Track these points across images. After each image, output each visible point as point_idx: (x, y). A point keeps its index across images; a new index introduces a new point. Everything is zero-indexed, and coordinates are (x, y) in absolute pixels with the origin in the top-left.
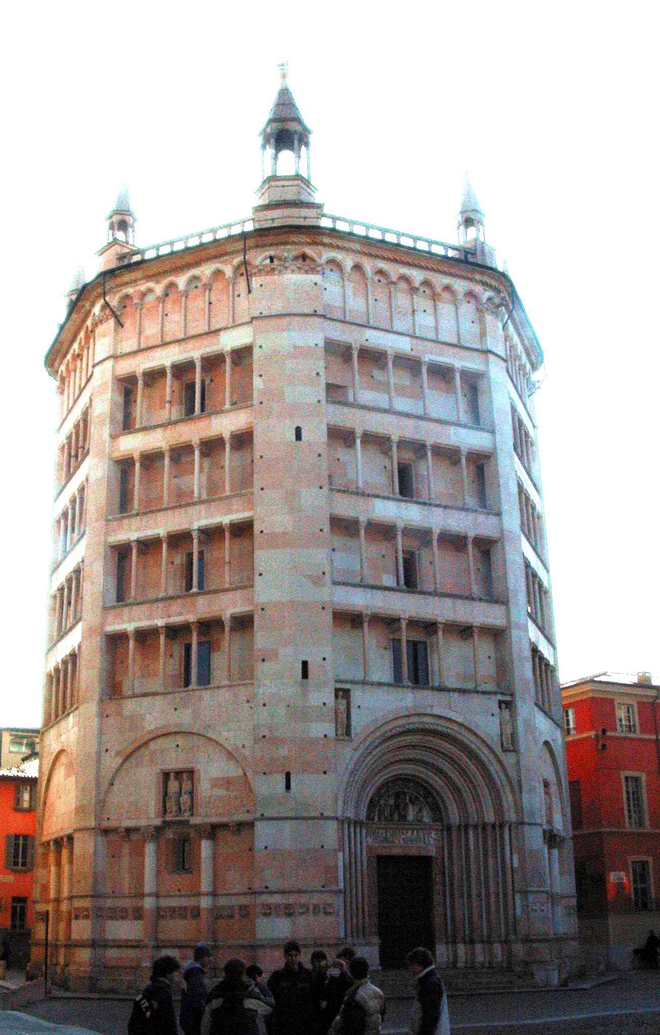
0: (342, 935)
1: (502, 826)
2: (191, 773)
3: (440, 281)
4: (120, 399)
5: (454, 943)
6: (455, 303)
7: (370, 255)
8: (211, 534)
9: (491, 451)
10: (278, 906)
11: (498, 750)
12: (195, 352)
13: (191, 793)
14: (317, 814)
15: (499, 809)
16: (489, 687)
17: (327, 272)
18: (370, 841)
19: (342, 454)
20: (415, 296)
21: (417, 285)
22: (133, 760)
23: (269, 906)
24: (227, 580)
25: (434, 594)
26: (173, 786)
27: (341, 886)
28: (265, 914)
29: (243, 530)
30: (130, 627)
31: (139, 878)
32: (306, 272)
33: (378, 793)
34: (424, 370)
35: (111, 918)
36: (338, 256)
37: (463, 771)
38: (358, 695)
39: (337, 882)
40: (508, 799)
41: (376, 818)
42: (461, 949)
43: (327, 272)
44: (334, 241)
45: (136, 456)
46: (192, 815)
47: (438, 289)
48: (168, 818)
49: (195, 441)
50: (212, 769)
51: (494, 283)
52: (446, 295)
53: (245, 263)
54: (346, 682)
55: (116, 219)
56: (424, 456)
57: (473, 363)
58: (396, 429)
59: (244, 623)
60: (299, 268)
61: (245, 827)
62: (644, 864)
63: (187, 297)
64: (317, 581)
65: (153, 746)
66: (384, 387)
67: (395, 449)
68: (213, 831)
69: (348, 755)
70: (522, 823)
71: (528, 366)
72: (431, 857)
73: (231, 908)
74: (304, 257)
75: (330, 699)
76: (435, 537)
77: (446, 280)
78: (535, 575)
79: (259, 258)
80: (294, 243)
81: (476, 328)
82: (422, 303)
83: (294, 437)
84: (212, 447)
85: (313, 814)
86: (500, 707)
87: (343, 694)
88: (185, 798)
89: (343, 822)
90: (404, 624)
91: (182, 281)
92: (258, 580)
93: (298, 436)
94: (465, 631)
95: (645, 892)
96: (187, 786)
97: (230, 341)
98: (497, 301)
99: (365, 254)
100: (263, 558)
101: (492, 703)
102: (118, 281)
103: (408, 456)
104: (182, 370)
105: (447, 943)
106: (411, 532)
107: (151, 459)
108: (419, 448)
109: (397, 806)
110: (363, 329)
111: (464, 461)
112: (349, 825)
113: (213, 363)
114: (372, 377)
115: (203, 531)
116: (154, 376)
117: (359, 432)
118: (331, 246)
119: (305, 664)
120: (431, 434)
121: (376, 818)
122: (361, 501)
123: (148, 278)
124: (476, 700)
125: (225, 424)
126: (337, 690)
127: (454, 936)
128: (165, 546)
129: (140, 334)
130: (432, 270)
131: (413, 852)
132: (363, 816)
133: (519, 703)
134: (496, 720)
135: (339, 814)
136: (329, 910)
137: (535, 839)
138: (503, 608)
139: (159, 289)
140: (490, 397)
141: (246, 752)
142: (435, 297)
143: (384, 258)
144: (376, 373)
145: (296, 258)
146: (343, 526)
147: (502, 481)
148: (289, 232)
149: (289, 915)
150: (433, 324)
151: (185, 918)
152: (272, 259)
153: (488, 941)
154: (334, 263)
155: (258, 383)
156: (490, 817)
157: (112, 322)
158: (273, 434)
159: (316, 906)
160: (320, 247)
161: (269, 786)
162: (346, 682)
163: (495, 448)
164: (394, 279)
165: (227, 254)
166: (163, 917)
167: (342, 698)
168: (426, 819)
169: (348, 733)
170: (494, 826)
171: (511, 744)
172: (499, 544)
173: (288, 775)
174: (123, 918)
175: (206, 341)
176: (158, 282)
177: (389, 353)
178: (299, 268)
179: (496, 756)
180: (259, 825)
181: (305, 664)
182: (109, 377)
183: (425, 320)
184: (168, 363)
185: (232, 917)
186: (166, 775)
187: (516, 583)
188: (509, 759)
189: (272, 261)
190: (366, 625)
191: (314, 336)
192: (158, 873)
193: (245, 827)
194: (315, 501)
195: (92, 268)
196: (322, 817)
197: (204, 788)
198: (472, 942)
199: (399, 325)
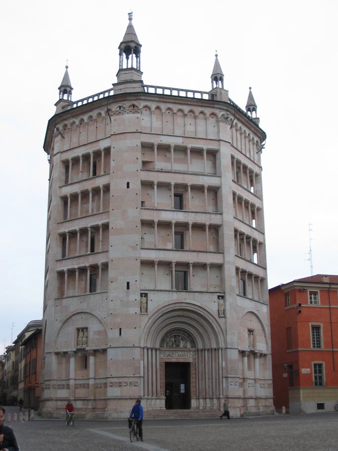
0: (142, 394)
1: (218, 349)
2: (87, 328)
3: (197, 110)
4: (63, 170)
5: (199, 399)
6: (206, 119)
7: (164, 102)
8: (96, 228)
9: (219, 185)
10: (116, 383)
11: (217, 317)
12: (90, 150)
13: (87, 337)
14: (132, 346)
15: (217, 342)
16: (217, 290)
17: (144, 112)
18: (162, 356)
19: (149, 191)
20: (186, 118)
21: (186, 113)
22: (66, 324)
23: (111, 383)
24: (101, 248)
25: (189, 251)
26: (81, 334)
27: (142, 375)
28: (111, 386)
29: (106, 227)
30: (65, 269)
31: (68, 373)
32: (134, 113)
33: (166, 335)
34: (189, 152)
35: (59, 389)
36: (148, 104)
37: (202, 325)
38: (151, 296)
39: (139, 373)
40: (221, 338)
41: (165, 346)
42: (201, 401)
43: (144, 112)
44: (146, 98)
45: (68, 195)
46: (87, 346)
47: (197, 114)
48: (79, 347)
49: (90, 189)
50: (94, 327)
51: (225, 108)
52: (201, 115)
53: (108, 110)
54: (146, 290)
55: (63, 89)
56: (187, 191)
57: (213, 146)
58: (173, 179)
59: (105, 266)
60: (131, 111)
61: (104, 351)
62: (320, 365)
63: (88, 125)
64: (134, 248)
65: (73, 318)
66: (168, 160)
67: (173, 188)
68: (95, 352)
69: (145, 321)
70: (227, 348)
71: (256, 139)
72: (189, 363)
73: (101, 384)
74: (134, 106)
75: (138, 297)
76: (190, 226)
77: (201, 109)
78: (248, 238)
79: (114, 107)
80: (128, 100)
81: (216, 129)
82: (189, 120)
83: (126, 187)
84: (96, 191)
85: (130, 346)
86: (219, 298)
87: (144, 295)
88: (84, 339)
89: (144, 348)
90: (174, 265)
91: (85, 118)
92: (110, 249)
93: (128, 187)
94: (203, 266)
95: (321, 378)
96: (86, 333)
97: (103, 145)
98: (226, 116)
99: (162, 102)
100: (113, 239)
101: (215, 297)
102: (62, 119)
103: (180, 191)
104: (86, 157)
105: (196, 399)
106: (178, 225)
107: (74, 197)
108: (185, 187)
109: (175, 341)
110: (159, 136)
111: (206, 191)
112: (148, 350)
113: (97, 154)
114: (166, 156)
115: (92, 227)
116: (76, 160)
117: (156, 182)
118: (145, 100)
119: (128, 283)
120: (190, 180)
121: (165, 346)
122: (155, 212)
123: (73, 117)
124: (206, 296)
125: (100, 182)
126: (141, 294)
127: (199, 396)
128: (78, 234)
129: (70, 142)
130: (194, 105)
131: (181, 360)
132: (158, 346)
133: (227, 297)
134: (216, 304)
135: (142, 346)
136: (136, 384)
137: (234, 355)
138: (221, 255)
139: (77, 122)
140: (220, 161)
141: (105, 320)
142: (195, 117)
143: (169, 102)
144: (167, 154)
145: (130, 106)
146: (147, 224)
147: (224, 199)
148: (129, 94)
149: (120, 386)
150: (194, 130)
151: (84, 387)
152: (120, 107)
153: (212, 399)
154: (147, 107)
155: (112, 164)
156: (214, 346)
157: (60, 136)
158: (117, 187)
159: (131, 383)
160: (140, 101)
161: (113, 334)
162: (146, 290)
163: (221, 184)
164: (175, 111)
165: (102, 106)
166: (77, 388)
167: (145, 297)
168: (189, 346)
169: (147, 312)
170: (215, 349)
171: (222, 314)
172: (221, 228)
173: (120, 329)
174: (63, 388)
175: (94, 145)
176: (77, 119)
177: (172, 145)
178: (131, 111)
179: (216, 320)
180: (109, 351)
181: (128, 283)
182: (58, 161)
183: (190, 129)
184: (80, 155)
185: (101, 387)
186: (78, 330)
187: (230, 243)
188: (221, 321)
189: (120, 109)
190: (156, 266)
191: (137, 141)
192: (76, 370)
193: (104, 351)
194: (136, 214)
195: (52, 111)
196: (134, 347)
197: (91, 334)
198: (206, 398)
199: (178, 132)
